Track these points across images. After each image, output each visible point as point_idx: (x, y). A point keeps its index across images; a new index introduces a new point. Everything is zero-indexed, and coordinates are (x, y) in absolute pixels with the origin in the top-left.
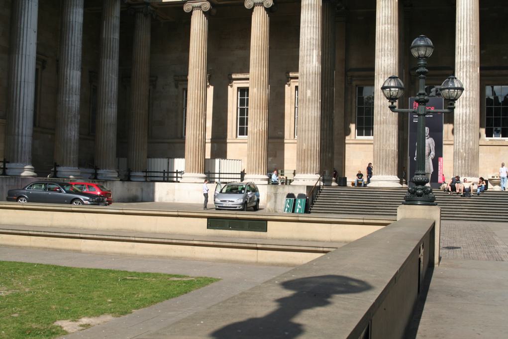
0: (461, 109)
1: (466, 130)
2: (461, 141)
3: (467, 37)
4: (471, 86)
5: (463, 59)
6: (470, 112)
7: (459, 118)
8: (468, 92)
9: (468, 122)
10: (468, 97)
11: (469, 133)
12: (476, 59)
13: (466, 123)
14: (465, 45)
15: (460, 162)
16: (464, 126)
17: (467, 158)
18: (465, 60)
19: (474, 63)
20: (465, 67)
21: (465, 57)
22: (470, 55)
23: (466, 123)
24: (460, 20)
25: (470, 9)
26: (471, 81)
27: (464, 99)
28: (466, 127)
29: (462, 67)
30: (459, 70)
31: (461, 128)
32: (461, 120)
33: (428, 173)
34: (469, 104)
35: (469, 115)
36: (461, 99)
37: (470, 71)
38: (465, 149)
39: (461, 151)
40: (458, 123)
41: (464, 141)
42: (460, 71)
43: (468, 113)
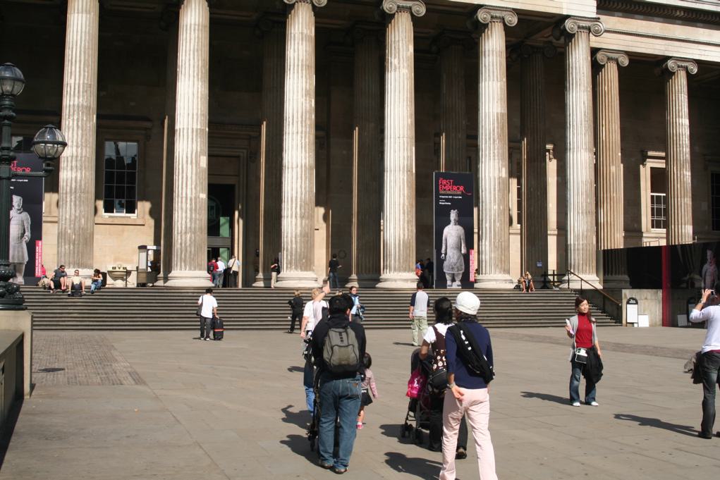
0: (69, 173)
1: (75, 201)
2: (68, 217)
3: (80, 72)
4: (83, 141)
5: (74, 101)
6: (81, 177)
7: (67, 185)
8: (79, 149)
9: (78, 191)
10: (79, 156)
11: (80, 206)
12: (92, 103)
13: (75, 192)
14: (77, 82)
15: (67, 247)
16: (73, 197)
17: (76, 242)
18: (76, 103)
19: (88, 108)
20: (76, 113)
21: (76, 98)
22: (83, 96)
23: (75, 192)
24: (71, 47)
25: (85, 32)
26: (84, 133)
27: (74, 158)
28: (75, 198)
29: (71, 113)
30: (67, 117)
31: (68, 200)
32: (68, 188)
33: (21, 264)
34: (81, 166)
35: (81, 180)
36: (70, 159)
37: (82, 119)
38: (75, 229)
39: (69, 231)
40: (64, 192)
41: (73, 217)
42: (69, 118)
43: (79, 178)
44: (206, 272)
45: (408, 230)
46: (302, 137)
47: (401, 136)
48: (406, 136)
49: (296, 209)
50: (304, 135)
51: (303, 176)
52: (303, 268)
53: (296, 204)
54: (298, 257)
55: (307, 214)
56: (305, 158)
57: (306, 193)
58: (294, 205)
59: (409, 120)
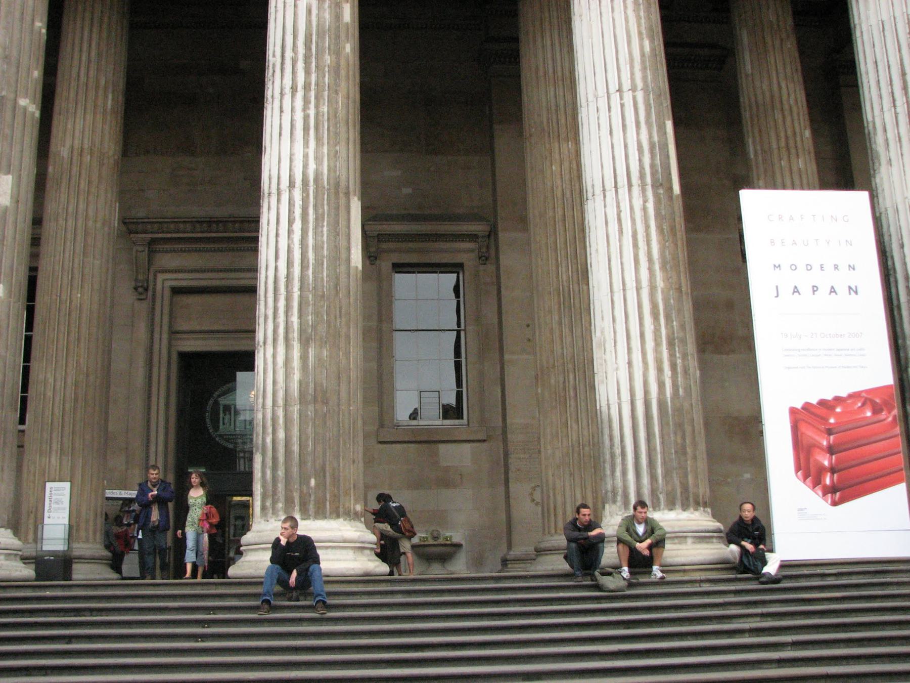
44: (102, 547)
45: (673, 367)
46: (306, 101)
47: (627, 85)
48: (640, 84)
49: (288, 308)
50: (313, 94)
51: (311, 211)
52: (311, 507)
53: (288, 299)
54: (295, 470)
55: (322, 329)
56: (319, 160)
57: (319, 263)
58: (282, 304)
59: (647, 43)
